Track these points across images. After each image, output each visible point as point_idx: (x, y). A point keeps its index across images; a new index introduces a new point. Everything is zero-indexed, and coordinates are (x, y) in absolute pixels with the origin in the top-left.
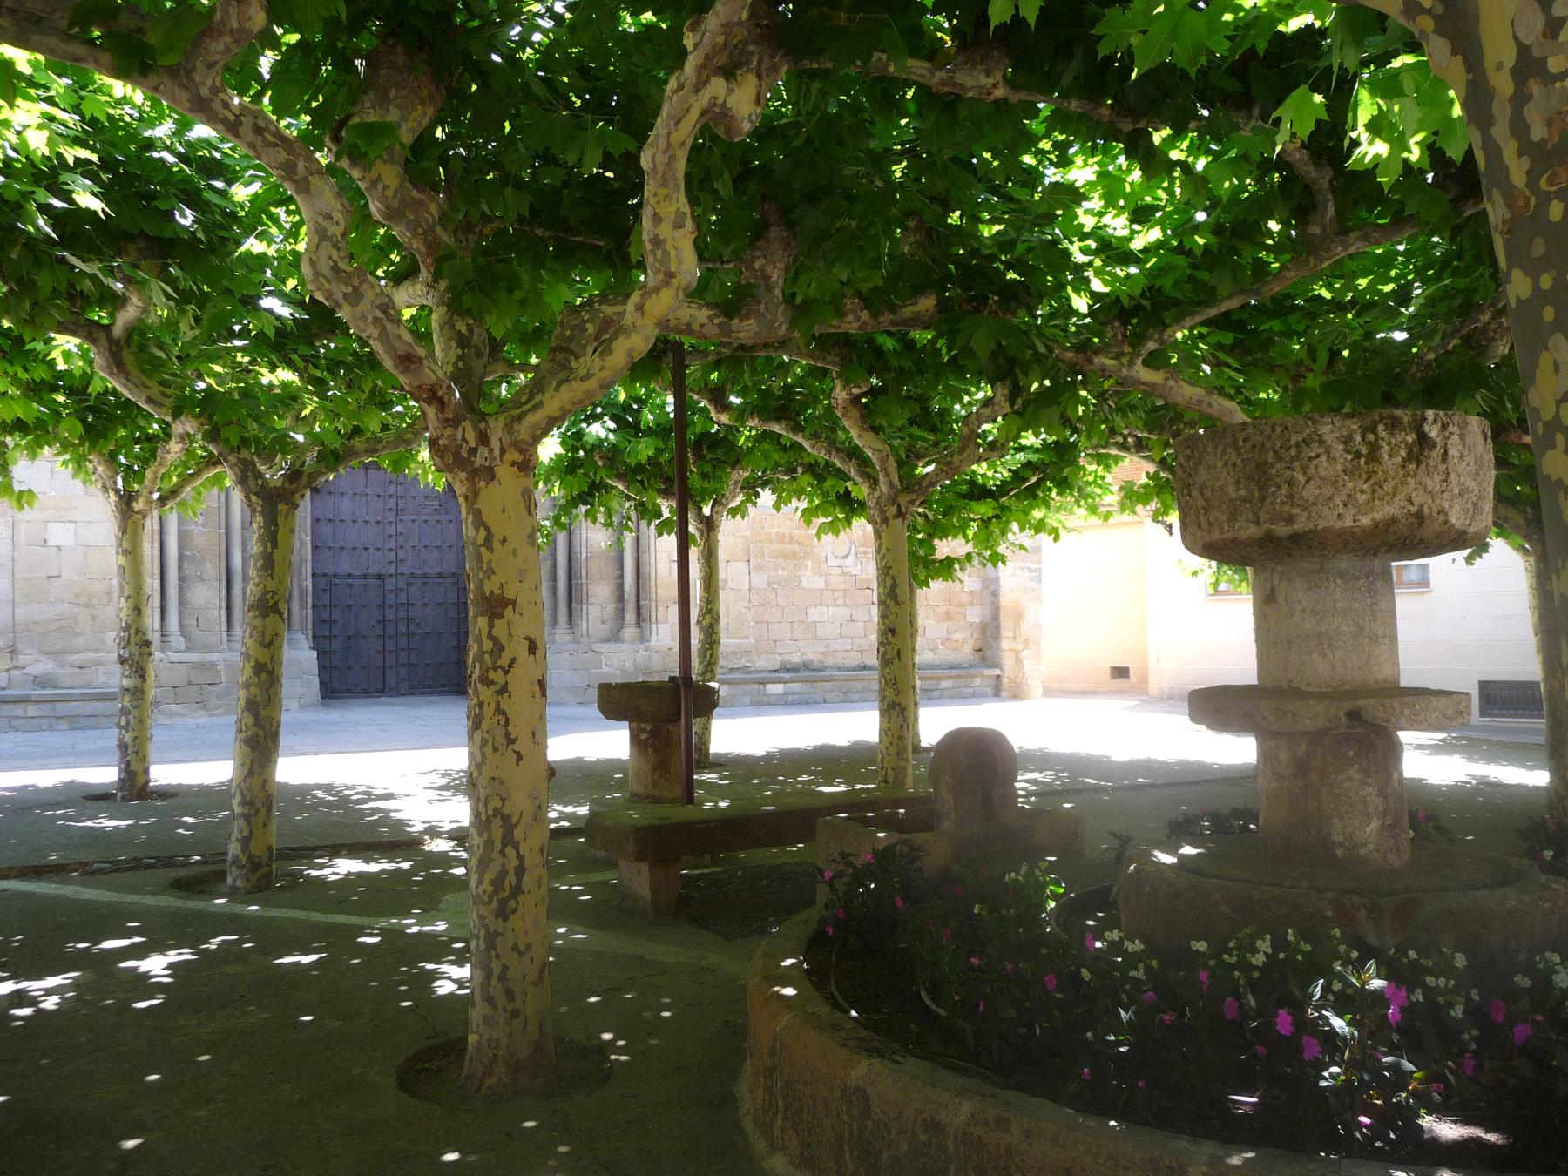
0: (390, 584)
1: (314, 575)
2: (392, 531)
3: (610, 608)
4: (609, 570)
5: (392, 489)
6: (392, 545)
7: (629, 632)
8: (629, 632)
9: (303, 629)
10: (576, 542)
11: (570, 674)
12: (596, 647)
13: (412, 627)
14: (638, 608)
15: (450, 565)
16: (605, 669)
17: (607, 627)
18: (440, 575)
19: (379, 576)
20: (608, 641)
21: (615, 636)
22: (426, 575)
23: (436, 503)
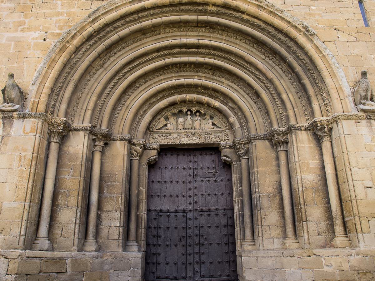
0: (189, 215)
1: (149, 211)
2: (190, 186)
3: (323, 224)
4: (319, 198)
5: (191, 165)
6: (191, 193)
7: (340, 240)
8: (340, 240)
9: (137, 240)
10: (294, 182)
11: (299, 271)
12: (315, 251)
13: (202, 241)
14: (344, 224)
15: (222, 203)
16: (326, 269)
17: (322, 237)
18: (217, 210)
19: (184, 211)
20: (324, 247)
21: (329, 244)
22: (209, 210)
23: (214, 171)
